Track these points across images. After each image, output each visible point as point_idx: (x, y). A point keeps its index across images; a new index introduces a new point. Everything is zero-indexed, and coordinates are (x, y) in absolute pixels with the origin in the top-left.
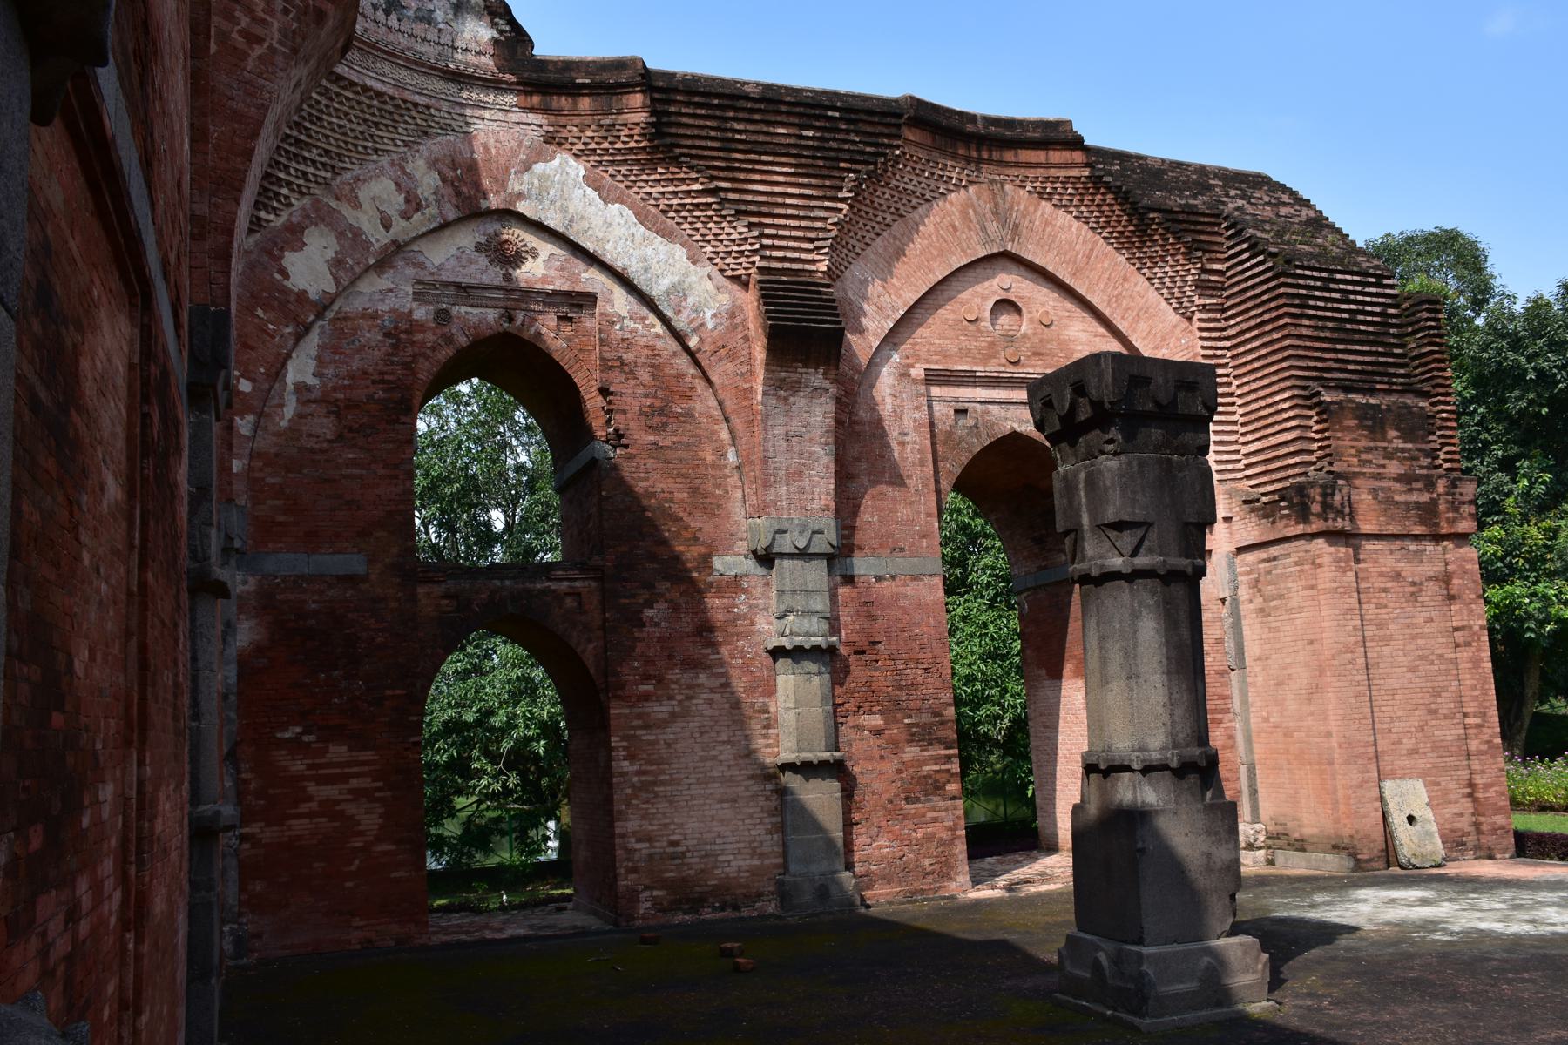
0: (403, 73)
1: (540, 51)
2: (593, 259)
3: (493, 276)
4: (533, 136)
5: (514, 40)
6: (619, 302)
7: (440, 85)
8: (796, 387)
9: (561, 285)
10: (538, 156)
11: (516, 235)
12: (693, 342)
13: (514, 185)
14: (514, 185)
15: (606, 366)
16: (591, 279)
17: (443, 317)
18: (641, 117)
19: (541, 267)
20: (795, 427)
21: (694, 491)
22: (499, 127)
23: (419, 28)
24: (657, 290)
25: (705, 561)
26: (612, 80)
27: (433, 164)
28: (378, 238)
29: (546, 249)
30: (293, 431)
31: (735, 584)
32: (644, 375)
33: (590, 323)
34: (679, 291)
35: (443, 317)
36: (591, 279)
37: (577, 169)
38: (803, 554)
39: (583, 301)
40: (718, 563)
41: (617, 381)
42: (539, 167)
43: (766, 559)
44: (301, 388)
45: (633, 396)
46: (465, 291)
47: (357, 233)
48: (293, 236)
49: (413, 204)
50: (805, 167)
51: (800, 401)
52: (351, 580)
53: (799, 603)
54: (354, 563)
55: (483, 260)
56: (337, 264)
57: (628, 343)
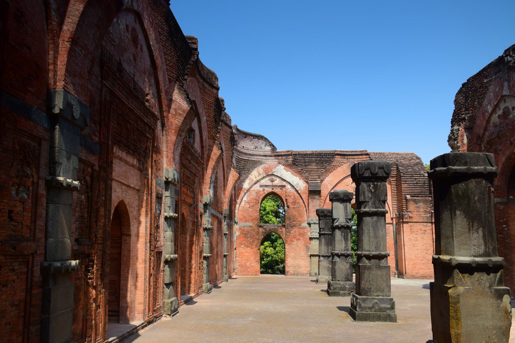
0: (258, 157)
1: (278, 150)
2: (285, 180)
3: (270, 184)
4: (277, 163)
5: (274, 148)
6: (289, 186)
7: (263, 157)
8: (314, 198)
9: (280, 184)
10: (277, 166)
11: (273, 177)
12: (299, 192)
13: (273, 170)
14: (273, 170)
15: (286, 196)
16: (284, 183)
17: (264, 190)
18: (291, 159)
19: (277, 182)
20: (314, 204)
21: (299, 214)
22: (271, 162)
23: (260, 150)
24: (294, 184)
25: (300, 225)
26: (287, 155)
27: (262, 168)
28: (255, 180)
29: (278, 179)
30: (244, 207)
31: (304, 228)
32: (292, 197)
33: (284, 189)
34: (297, 184)
35: (264, 190)
36: (284, 183)
37: (283, 167)
38: (315, 223)
39: (284, 186)
40: (302, 224)
41: (288, 198)
42: (277, 167)
43: (309, 224)
44: (245, 201)
45: (290, 200)
46: (266, 186)
47: (252, 179)
48: (244, 181)
49: (260, 174)
50: (317, 164)
51: (315, 201)
52: (251, 226)
53: (314, 231)
54: (251, 224)
55: (269, 181)
56: (249, 184)
57: (290, 192)
